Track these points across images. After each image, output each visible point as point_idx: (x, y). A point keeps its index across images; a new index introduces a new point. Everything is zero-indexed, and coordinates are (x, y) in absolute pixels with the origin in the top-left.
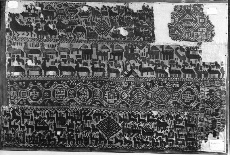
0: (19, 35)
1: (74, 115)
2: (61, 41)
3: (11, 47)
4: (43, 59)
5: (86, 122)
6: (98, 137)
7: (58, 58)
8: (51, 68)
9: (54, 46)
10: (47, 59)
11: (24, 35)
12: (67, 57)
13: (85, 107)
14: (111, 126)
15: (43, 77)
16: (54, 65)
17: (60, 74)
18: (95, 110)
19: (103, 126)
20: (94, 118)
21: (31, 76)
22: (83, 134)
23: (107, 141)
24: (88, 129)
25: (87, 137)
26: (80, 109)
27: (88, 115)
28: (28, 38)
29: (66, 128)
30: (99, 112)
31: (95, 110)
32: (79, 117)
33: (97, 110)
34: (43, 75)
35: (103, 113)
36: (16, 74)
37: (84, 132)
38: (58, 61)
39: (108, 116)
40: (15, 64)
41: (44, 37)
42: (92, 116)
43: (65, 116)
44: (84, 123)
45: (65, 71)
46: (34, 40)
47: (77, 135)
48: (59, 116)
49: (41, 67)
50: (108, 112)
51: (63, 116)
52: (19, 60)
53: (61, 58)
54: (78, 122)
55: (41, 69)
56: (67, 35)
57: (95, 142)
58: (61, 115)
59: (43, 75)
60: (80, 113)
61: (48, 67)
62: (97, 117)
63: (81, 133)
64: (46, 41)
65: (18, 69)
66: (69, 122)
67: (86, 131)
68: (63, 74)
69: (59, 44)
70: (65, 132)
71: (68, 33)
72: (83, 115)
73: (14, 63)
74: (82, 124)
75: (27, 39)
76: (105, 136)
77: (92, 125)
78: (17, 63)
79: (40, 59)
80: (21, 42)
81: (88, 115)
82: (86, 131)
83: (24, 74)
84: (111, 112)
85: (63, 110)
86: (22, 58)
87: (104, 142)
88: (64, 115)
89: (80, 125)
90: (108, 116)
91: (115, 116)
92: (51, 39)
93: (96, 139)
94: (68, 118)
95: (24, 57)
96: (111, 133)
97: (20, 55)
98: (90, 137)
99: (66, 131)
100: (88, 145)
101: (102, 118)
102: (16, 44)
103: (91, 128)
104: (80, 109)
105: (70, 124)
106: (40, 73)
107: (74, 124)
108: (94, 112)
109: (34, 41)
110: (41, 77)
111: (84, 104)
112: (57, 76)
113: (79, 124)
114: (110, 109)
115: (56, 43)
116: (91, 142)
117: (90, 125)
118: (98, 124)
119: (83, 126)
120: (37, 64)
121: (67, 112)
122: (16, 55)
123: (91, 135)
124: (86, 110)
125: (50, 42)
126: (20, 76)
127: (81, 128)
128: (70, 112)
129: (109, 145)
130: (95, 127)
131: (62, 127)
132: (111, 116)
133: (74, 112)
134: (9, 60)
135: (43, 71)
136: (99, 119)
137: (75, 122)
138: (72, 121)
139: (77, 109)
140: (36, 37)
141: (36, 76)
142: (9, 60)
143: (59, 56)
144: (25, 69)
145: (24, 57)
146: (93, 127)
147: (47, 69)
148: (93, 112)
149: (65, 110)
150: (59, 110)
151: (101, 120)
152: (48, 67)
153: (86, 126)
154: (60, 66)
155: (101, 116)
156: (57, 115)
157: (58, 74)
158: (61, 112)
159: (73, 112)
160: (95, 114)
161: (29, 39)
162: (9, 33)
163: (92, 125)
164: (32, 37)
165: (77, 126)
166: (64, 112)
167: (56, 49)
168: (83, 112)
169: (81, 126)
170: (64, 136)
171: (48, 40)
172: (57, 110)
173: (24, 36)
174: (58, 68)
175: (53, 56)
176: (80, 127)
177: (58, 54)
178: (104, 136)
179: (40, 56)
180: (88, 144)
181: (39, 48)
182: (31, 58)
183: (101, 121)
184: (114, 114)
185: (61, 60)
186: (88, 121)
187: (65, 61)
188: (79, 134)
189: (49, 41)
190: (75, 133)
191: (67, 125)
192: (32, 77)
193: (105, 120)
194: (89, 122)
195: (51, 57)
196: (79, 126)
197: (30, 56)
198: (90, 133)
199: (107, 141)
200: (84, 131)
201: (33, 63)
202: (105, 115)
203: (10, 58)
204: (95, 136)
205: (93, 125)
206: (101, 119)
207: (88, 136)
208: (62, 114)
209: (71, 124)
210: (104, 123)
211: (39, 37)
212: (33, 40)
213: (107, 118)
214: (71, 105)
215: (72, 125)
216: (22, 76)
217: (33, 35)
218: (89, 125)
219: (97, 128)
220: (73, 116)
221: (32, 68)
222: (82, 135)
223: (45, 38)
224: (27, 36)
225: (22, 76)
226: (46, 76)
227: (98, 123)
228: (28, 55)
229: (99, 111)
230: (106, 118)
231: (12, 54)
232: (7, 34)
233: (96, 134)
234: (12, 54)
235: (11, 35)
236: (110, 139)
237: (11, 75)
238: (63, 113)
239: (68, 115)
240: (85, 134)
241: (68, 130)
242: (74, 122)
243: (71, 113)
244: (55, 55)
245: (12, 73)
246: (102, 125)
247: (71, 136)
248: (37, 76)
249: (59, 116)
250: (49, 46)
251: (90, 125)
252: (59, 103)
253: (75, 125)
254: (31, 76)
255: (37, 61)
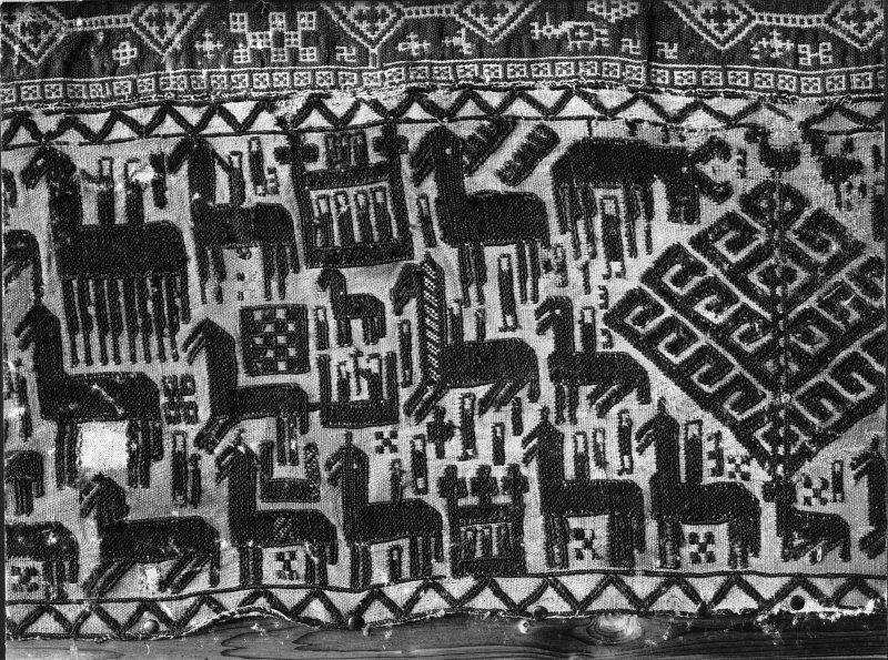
1: (301, 181)
5: (473, 273)
6: (645, 465)
13: (444, 71)
14: (809, 313)
18: (576, 106)
19: (698, 320)
20: (577, 209)
22: (440, 433)
23: (769, 513)
24: (502, 366)
25: (499, 473)
26: (376, 106)
27: (485, 180)
29: (200, 371)
30: (633, 125)
31: (576, 106)
32: (364, 218)
33: (610, 98)
35: (694, 143)
37: (453, 415)
39: (759, 172)
42: (540, 181)
43: (178, 211)
44: (440, 294)
47: (352, 465)
48: (90, 214)
50: (763, 116)
51: (152, 213)
54: (359, 282)
57: (601, 543)
58: (120, 204)
60: (374, 158)
62: (610, 198)
63: (408, 431)
66: (231, 287)
67: (481, 391)
70: (193, 431)
72: (418, 180)
74: (411, 310)
76: (732, 446)
77: (557, 315)
81: (485, 180)
82: (481, 391)
84: (799, 115)
85: (144, 132)
87: (721, 531)
88: (161, 202)
89: (391, 320)
90: (759, 172)
91: (857, 167)
93: (618, 500)
94: (221, 229)
96: (811, 399)
98: (531, 472)
99: (204, 413)
100: (507, 584)
101: (684, 210)
103: (544, 346)
104: (376, 106)
105: (246, 314)
107: (297, 313)
108: (570, 132)
111: (418, 27)
113: (368, 308)
114: (787, 81)
116: (557, 536)
117: (527, 311)
118: (633, 298)
119: (423, 327)
121: (195, 154)
123: (546, 443)
124: (451, 114)
127: (408, 365)
128: (242, 144)
129: (793, 567)
130: (589, 332)
131: (140, 366)
132: (807, 177)
133: (296, 154)
136: (641, 224)
137: (322, 282)
138: (278, 268)
139: (339, 104)
146: (564, 339)
148: (554, 140)
149: (170, 126)
150: (85, 131)
151: (668, 233)
153: (470, 334)
155: (659, 189)
156: (65, 205)
158: (114, 151)
159: (282, 141)
160: (593, 162)
163: (557, 315)
165: (345, 338)
166: (156, 161)
168: (414, 135)
169: (405, 340)
170: (178, 484)
172: (63, 127)
176: (388, 345)
178: (717, 455)
180: (514, 563)
183: (674, 253)
184: (835, 146)
186: (492, 253)
188: (387, 444)
190: (329, 440)
191: (209, 335)
193: (717, 230)
194: (505, 281)
196: (375, 333)
198: (531, 420)
199: (769, 513)
200: (452, 402)
202: (719, 170)
204: (602, 464)
205: (564, 304)
206: (673, 216)
207: (499, 456)
208: (135, 189)
209: (269, 313)
210: (712, 270)
213: (748, 201)
214: (243, 54)
215: (277, 335)
218: (508, 306)
219: (622, 345)
220: (285, 198)
222: (419, 460)
227: (633, 282)
229: (640, 111)
230: (732, 205)
233: (611, 425)
236: (802, 492)
238: (147, 176)
239: (223, 195)
240: (469, 441)
241: (232, 405)
242: (305, 286)
243: (257, 159)
246: (684, 305)
247: (281, 472)
249: (90, 214)
251: (527, 311)
252: (87, 38)
253: (322, 327)
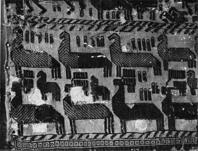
0: (44, 11)
2: (169, 27)
3: (22, 47)
4: (116, 82)
7: (162, 81)
8: (144, 111)
9: (148, 43)
10: (127, 81)
11: (59, 9)
12: (187, 77)
15: (118, 136)
16: (150, 99)
17: (166, 127)
21: (82, 135)
28: (72, 20)
34: (118, 129)
36: (40, 128)
38: (160, 88)
40: (35, 98)
41: (118, 17)
45: (181, 118)
46: (91, 25)
49: (111, 109)
52: (45, 88)
53: (170, 79)
55: (110, 115)
56: (186, 10)
59: (118, 129)
61: (131, 107)
64: (125, 27)
65: (45, 114)
68: (177, 128)
69: (163, 38)
71: (189, 4)
73: (29, 95)
75: (69, 23)
78: (40, 96)
79: (108, 83)
80: (49, 32)
83: (61, 130)
86: (53, 80)
92: (141, 22)
95: (60, 77)
97: (48, 71)
102: (36, 38)
106: (109, 126)
109: (89, 29)
110: (112, 137)
112: (158, 135)
115: (156, 36)
120: (101, 97)
122: (36, 71)
125: (138, 30)
126: (48, 137)
134: (16, 87)
135: (117, 120)
140: (94, 18)
141: (98, 134)
142: (16, 87)
143: (165, 74)
144: (63, 113)
145: (60, 77)
147: (127, 114)
152: (131, 107)
154: (167, 102)
157: (160, 128)
161: (74, 23)
162: (14, 5)
164: (83, 18)
167: (155, 50)
171: (131, 25)
173: (59, 15)
174: (161, 110)
175: (145, 74)
177: (162, 68)
179: (107, 74)
181: (105, 52)
182: (80, 80)
185: (171, 85)
187: (181, 87)
189: (134, 27)
192: (84, 137)
195: (139, 75)
197: (77, 75)
201: (86, 94)
203: (16, 79)
211: (105, 18)
212: (86, 27)
216: (54, 136)
217: (86, 12)
221: (84, 112)
223: (123, 20)
224: (69, 13)
225: (54, 136)
226: (127, 136)
228: (73, 71)
231: (23, 68)
232: (10, 7)
234: (23, 68)
235: (19, 11)
237: (21, 132)
244: (151, 71)
245: (25, 126)
248: (101, 136)
250: (133, 42)
254: (82, 135)
255: (100, 92)
